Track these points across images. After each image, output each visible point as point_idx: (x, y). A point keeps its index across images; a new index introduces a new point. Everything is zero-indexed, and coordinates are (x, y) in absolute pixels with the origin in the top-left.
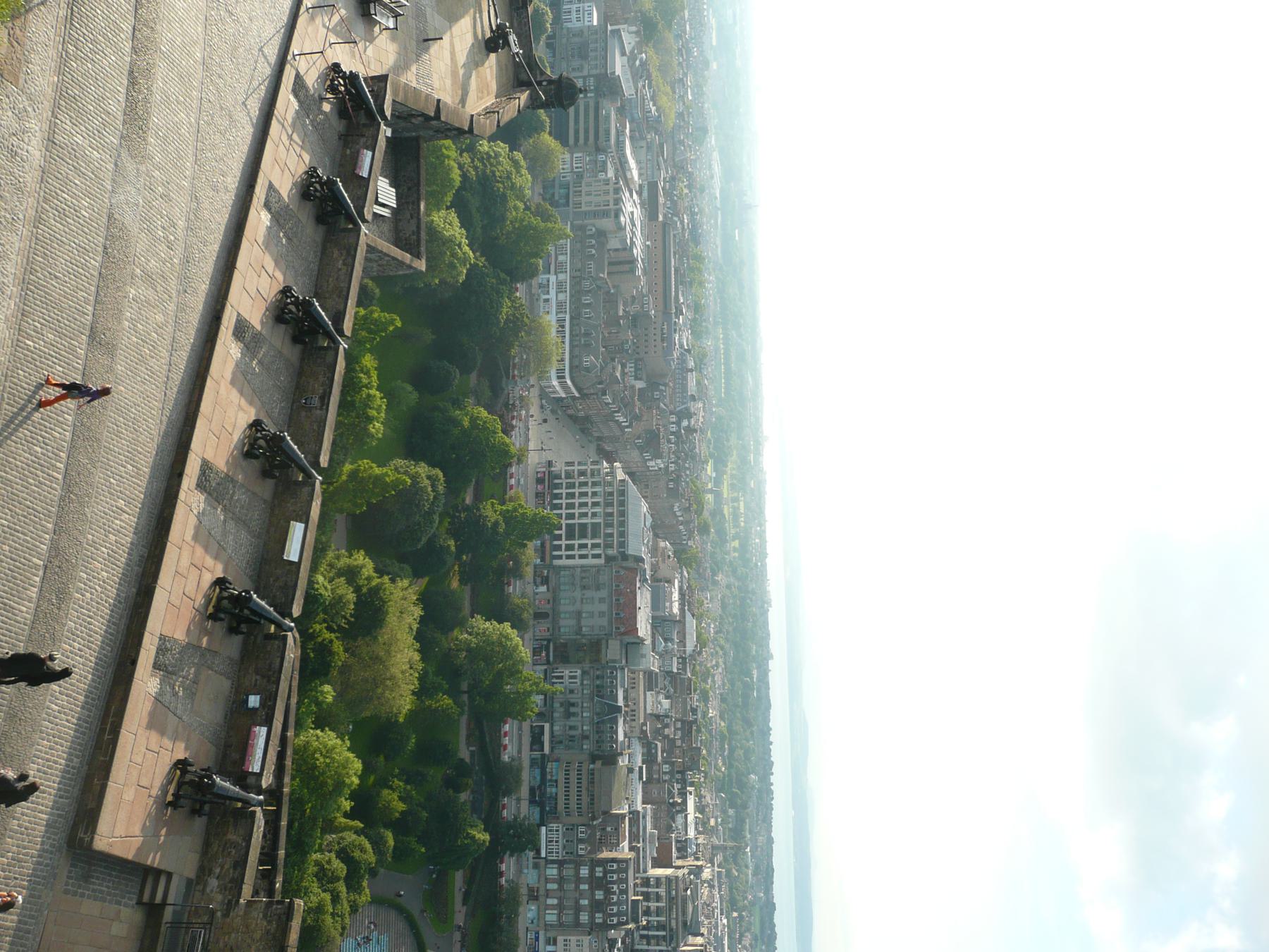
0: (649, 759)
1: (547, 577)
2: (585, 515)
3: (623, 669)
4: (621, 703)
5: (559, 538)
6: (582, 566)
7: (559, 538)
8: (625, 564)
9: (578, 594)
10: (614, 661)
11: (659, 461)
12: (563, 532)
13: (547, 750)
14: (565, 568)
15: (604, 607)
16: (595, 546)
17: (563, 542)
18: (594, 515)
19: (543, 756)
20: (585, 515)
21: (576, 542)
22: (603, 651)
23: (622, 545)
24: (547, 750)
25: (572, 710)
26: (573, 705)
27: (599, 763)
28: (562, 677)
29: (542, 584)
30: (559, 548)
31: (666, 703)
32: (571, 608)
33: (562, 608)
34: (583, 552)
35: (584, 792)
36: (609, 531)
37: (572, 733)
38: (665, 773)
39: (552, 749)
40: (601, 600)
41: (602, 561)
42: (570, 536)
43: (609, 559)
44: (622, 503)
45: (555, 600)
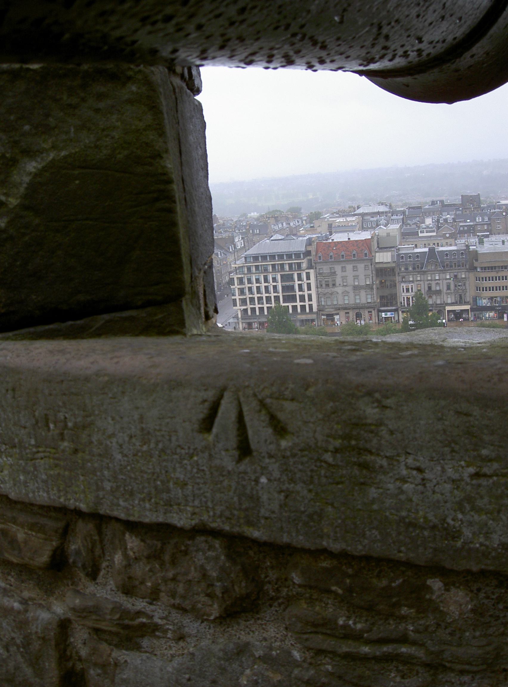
0: (471, 231)
1: (328, 315)
2: (275, 287)
3: (399, 249)
4: (426, 250)
5: (294, 308)
6: (317, 287)
7: (294, 308)
8: (313, 253)
9: (339, 290)
10: (392, 257)
11: (236, 240)
12: (290, 305)
13: (467, 307)
14: (319, 301)
15: (349, 267)
16: (300, 278)
17: (298, 304)
18: (274, 280)
19: (472, 309)
20: (275, 287)
21: (298, 293)
22: (385, 266)
23: (298, 255)
24: (467, 307)
25: (433, 289)
26: (430, 288)
27: (476, 264)
28: (408, 299)
29: (333, 320)
30: (303, 307)
31: (429, 221)
32: (352, 294)
33: (352, 302)
34: (305, 287)
35: (501, 274)
36: (287, 267)
37: (452, 287)
38: (483, 219)
39: (466, 303)
40: (344, 269)
41: (312, 272)
42: (293, 298)
43: (310, 267)
44: (264, 258)
45: (346, 308)
